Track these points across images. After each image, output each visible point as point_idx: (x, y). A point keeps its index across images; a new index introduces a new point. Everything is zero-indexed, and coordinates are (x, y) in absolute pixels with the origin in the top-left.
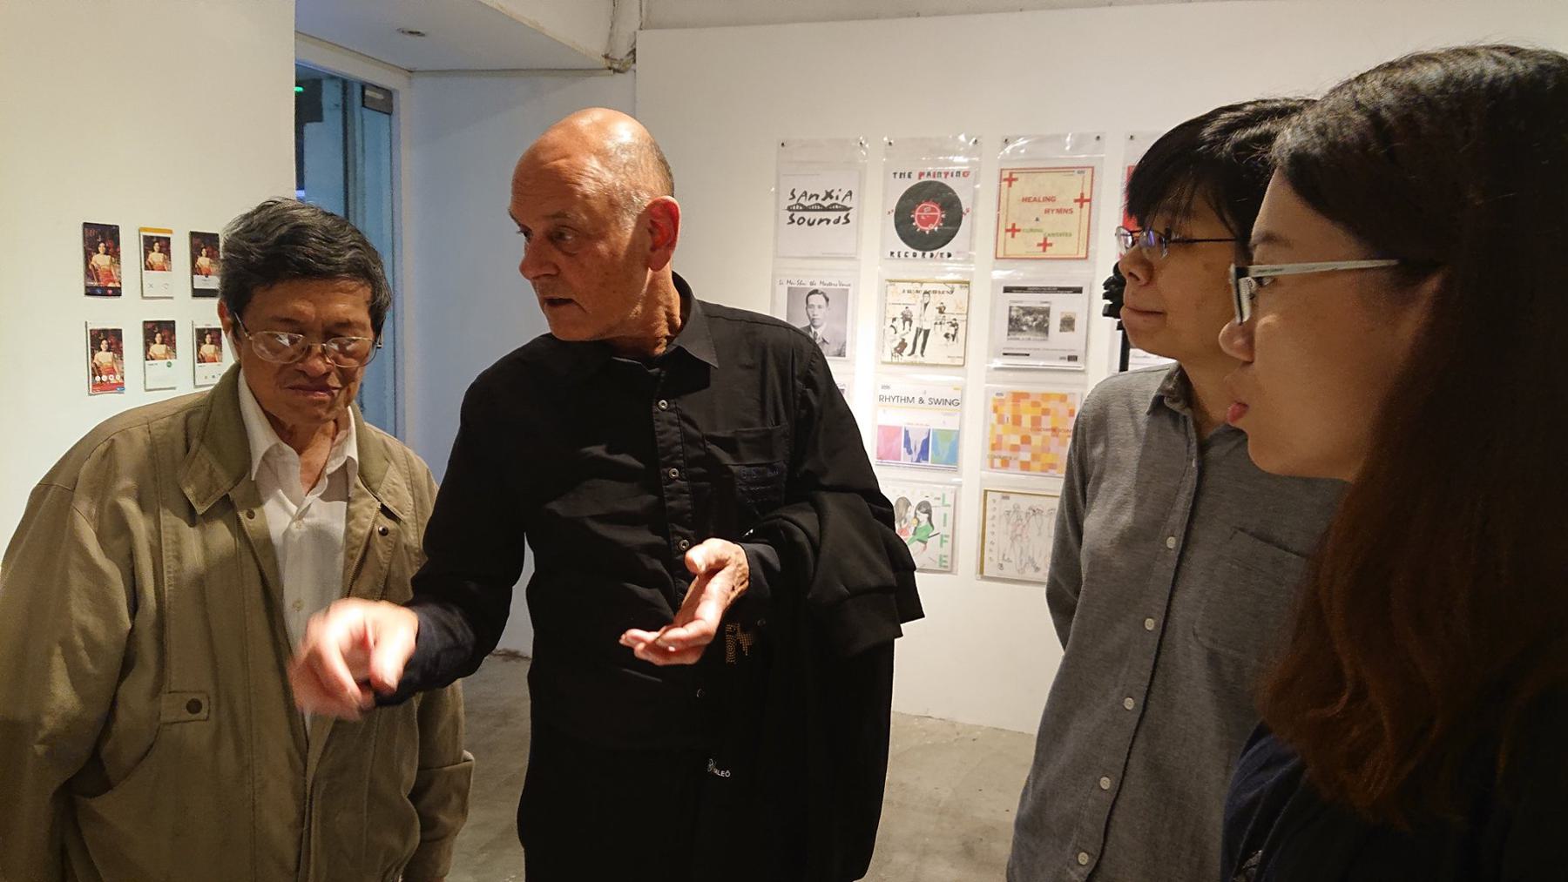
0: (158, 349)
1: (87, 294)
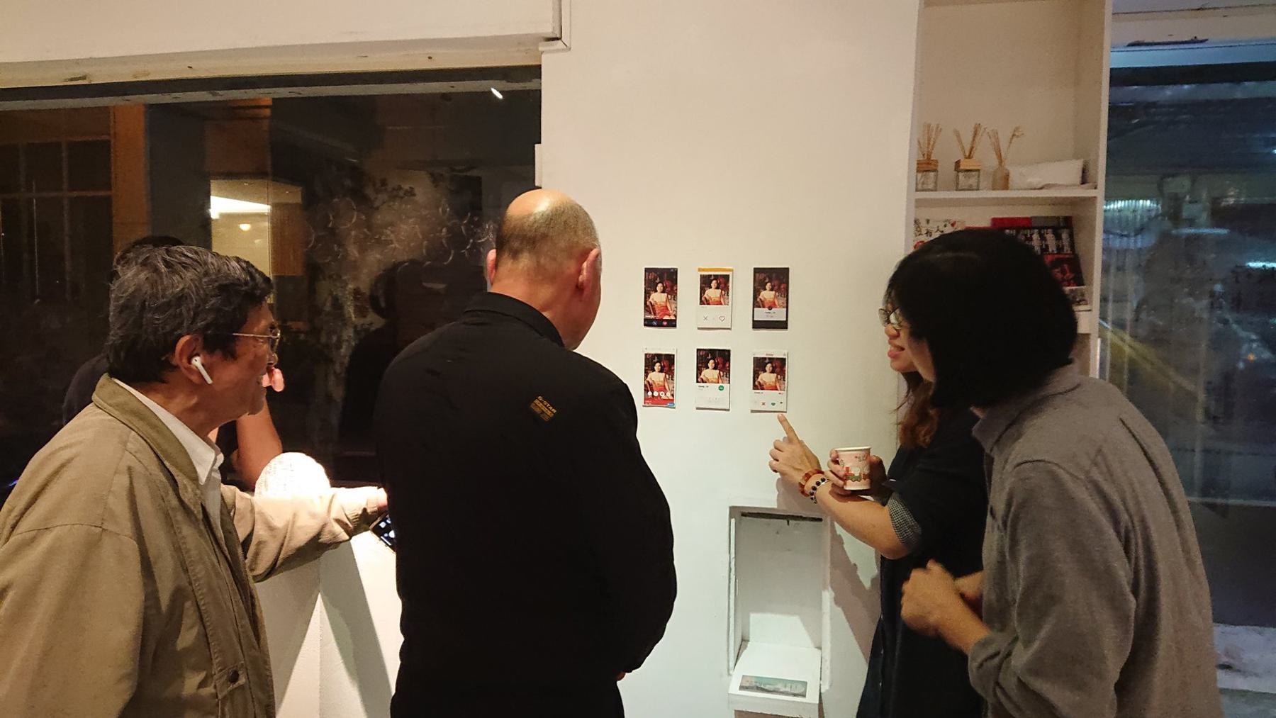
0: (710, 373)
1: (645, 325)
